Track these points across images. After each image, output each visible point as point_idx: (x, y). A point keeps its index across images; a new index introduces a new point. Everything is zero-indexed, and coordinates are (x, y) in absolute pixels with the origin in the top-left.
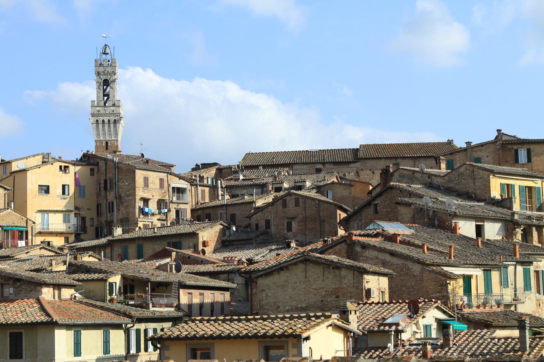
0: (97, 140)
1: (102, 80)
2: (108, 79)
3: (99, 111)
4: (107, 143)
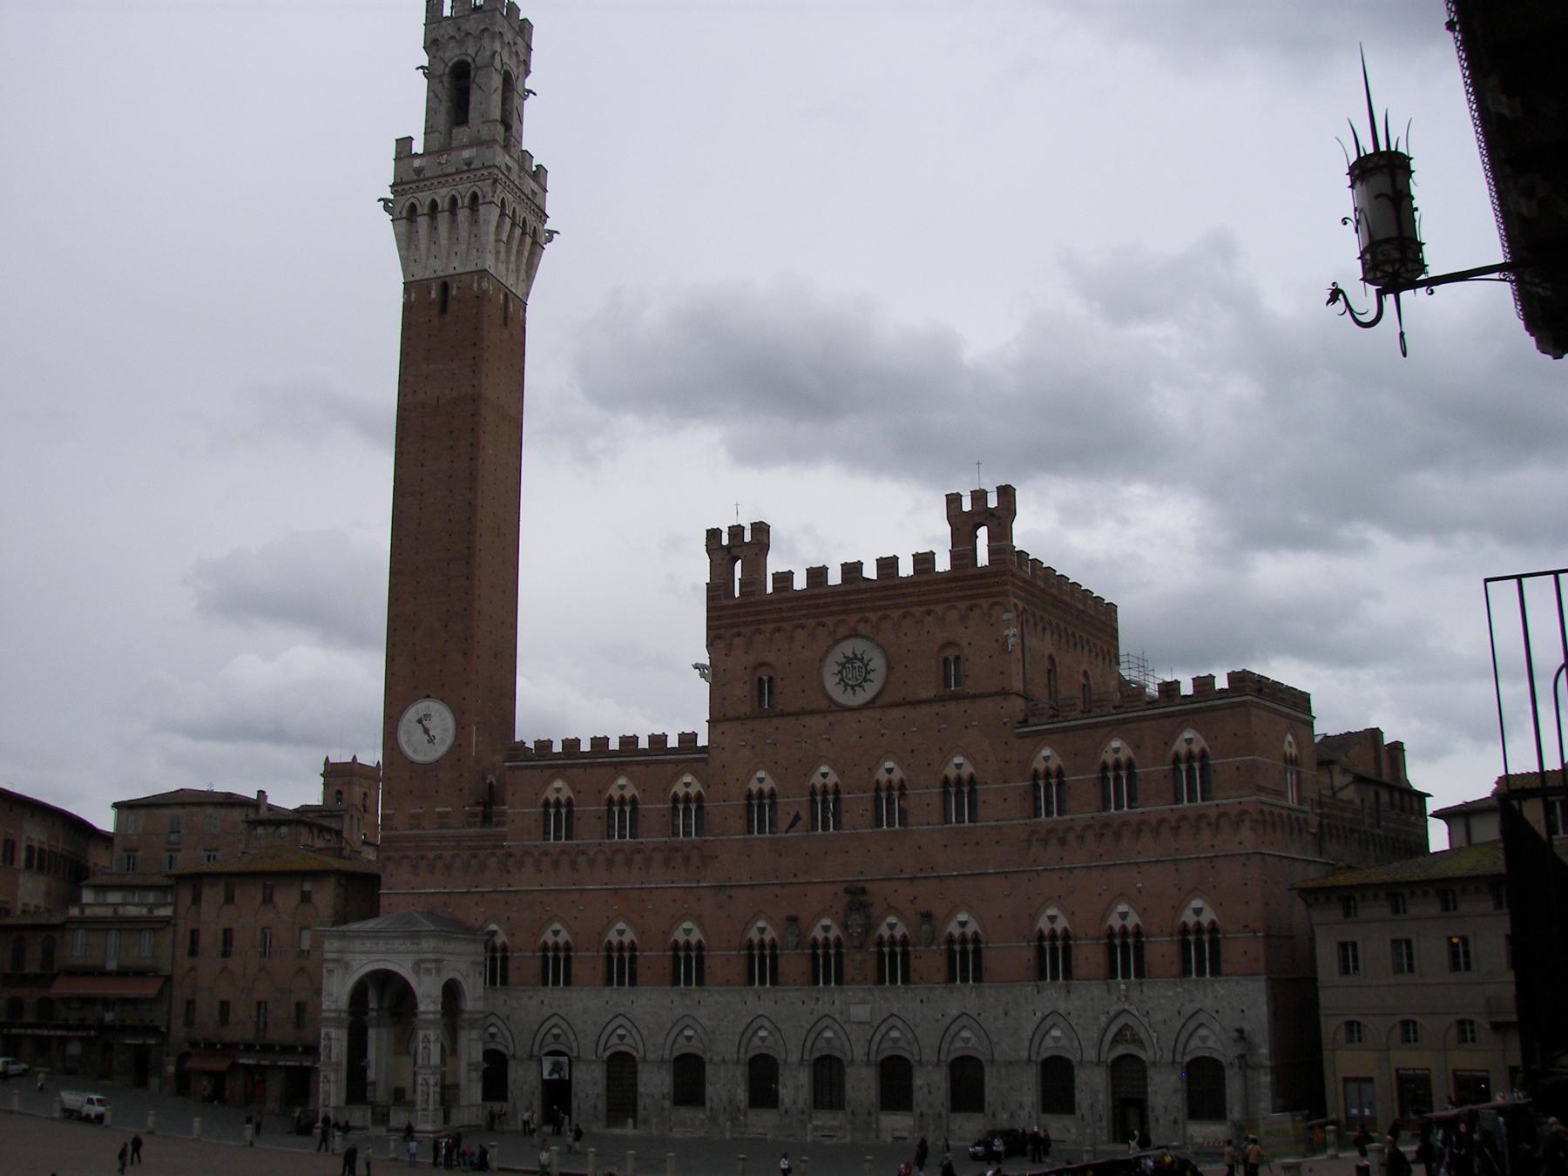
0: (411, 282)
1: (447, 65)
2: (470, 60)
3: (419, 171)
4: (445, 288)
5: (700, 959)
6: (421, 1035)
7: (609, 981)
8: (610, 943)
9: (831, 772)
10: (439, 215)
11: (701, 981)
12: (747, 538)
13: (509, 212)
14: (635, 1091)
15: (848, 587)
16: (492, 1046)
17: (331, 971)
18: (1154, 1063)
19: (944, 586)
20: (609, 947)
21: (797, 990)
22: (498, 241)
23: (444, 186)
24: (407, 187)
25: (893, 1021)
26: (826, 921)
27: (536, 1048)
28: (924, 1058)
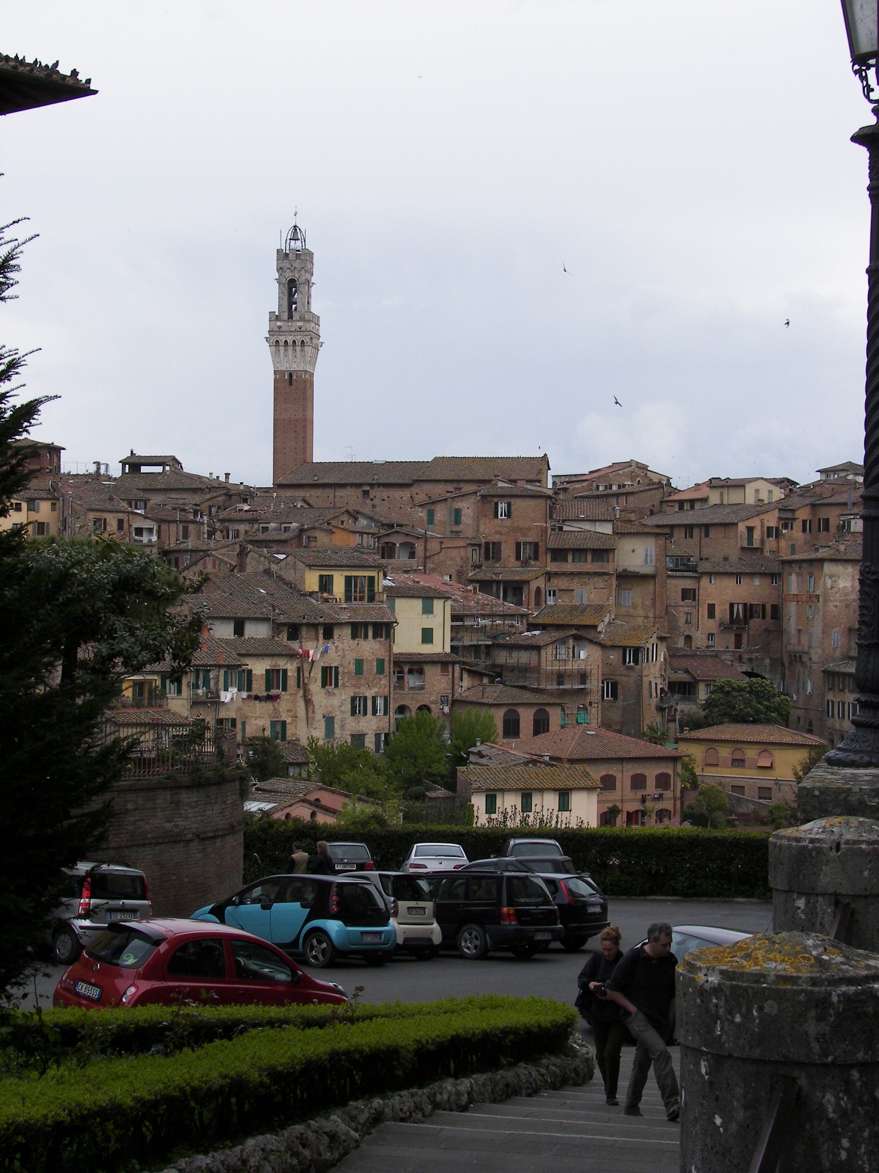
3: (280, 327)
4: (291, 375)
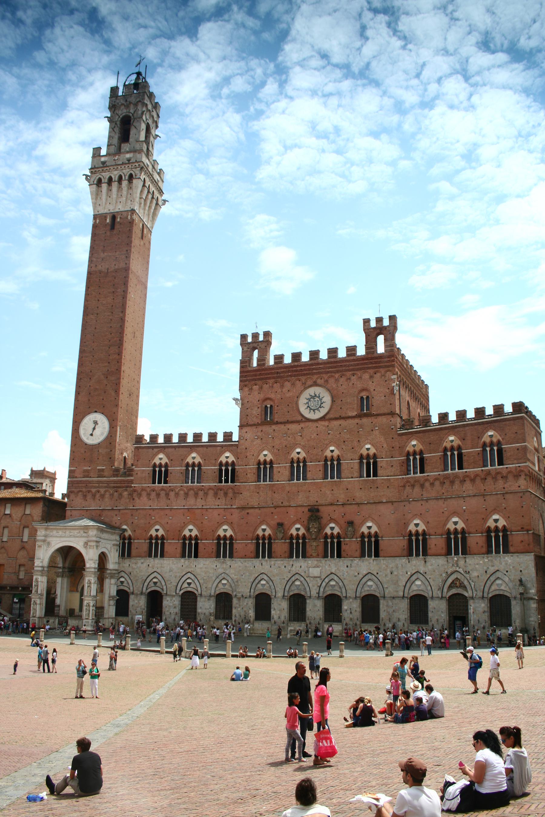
1: (119, 117)
2: (131, 115)
3: (104, 163)
4: (114, 218)
5: (231, 544)
6: (87, 579)
7: (183, 556)
8: (185, 536)
9: (302, 452)
10: (113, 183)
11: (231, 556)
12: (261, 338)
13: (147, 185)
14: (196, 612)
15: (313, 362)
16: (122, 588)
17: (40, 546)
18: (472, 598)
19: (362, 362)
20: (184, 538)
21: (282, 560)
22: (140, 198)
23: (116, 170)
24: (97, 170)
25: (332, 576)
26: (298, 526)
27: (144, 589)
28: (348, 595)
